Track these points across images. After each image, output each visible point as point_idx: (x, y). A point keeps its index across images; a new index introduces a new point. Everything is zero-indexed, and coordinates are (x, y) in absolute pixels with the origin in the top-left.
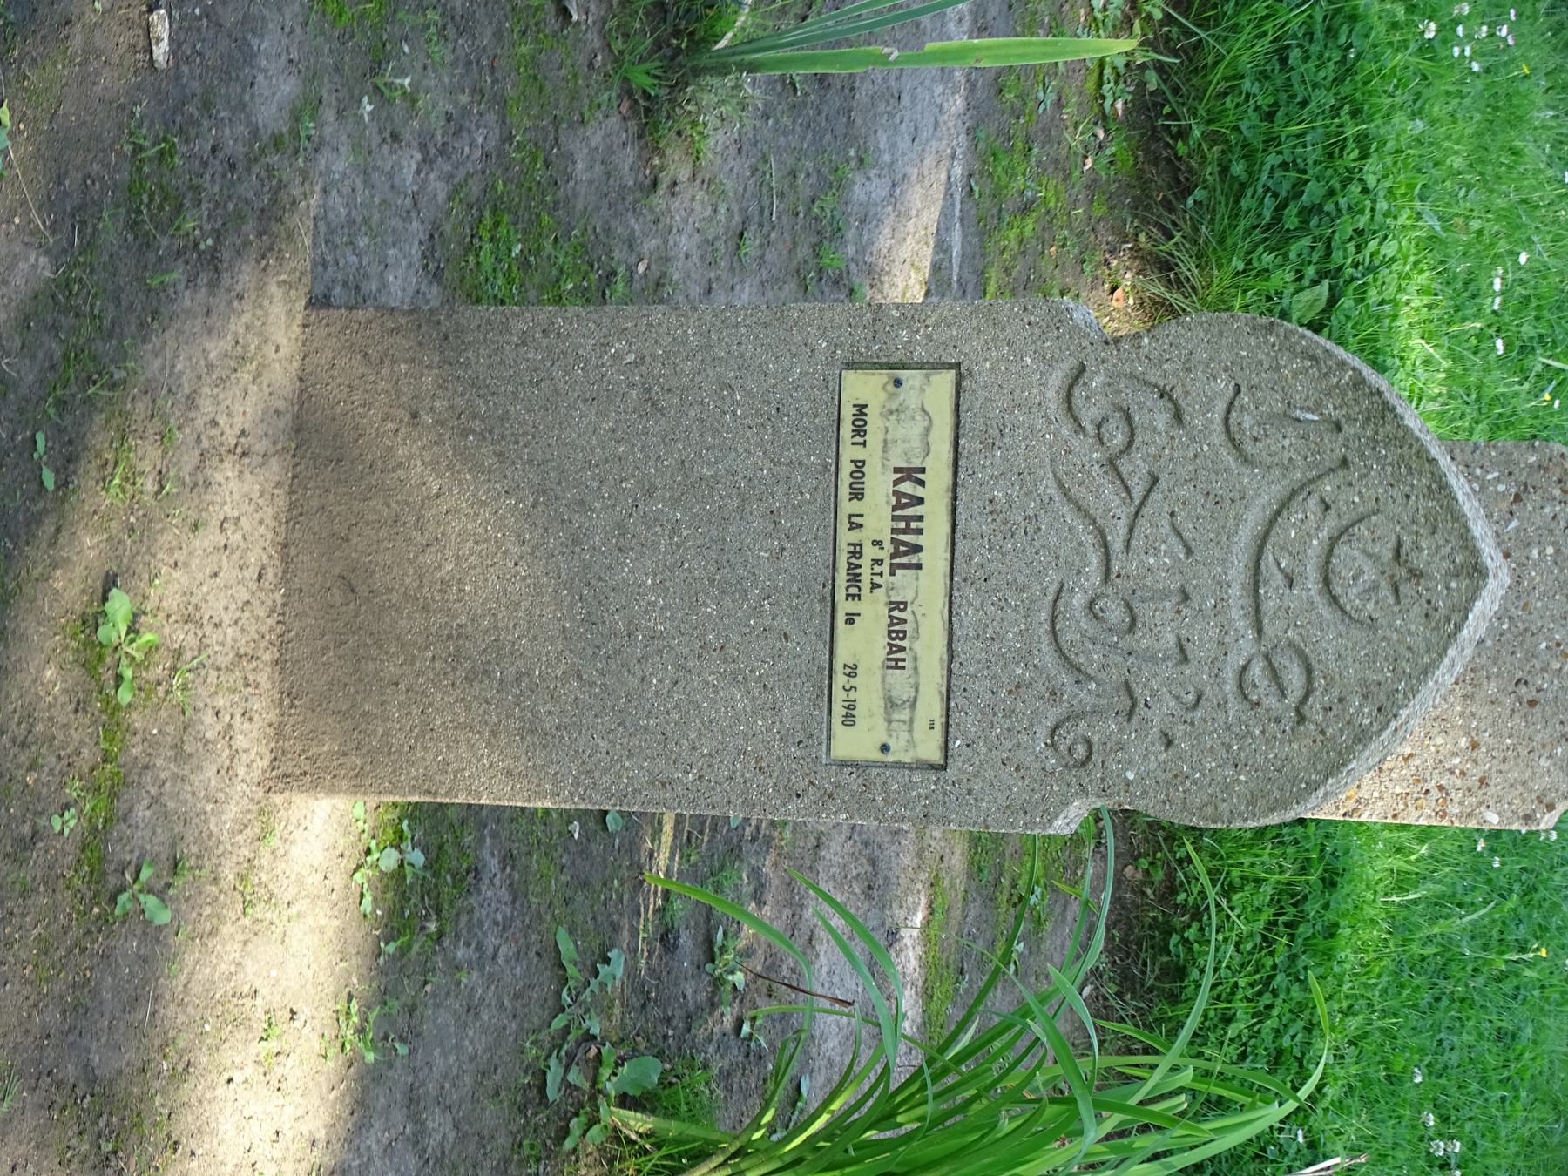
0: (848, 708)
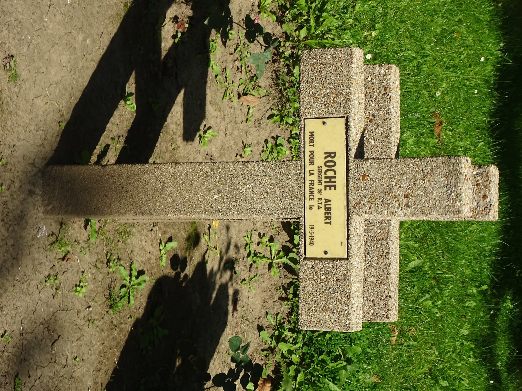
0: (311, 239)
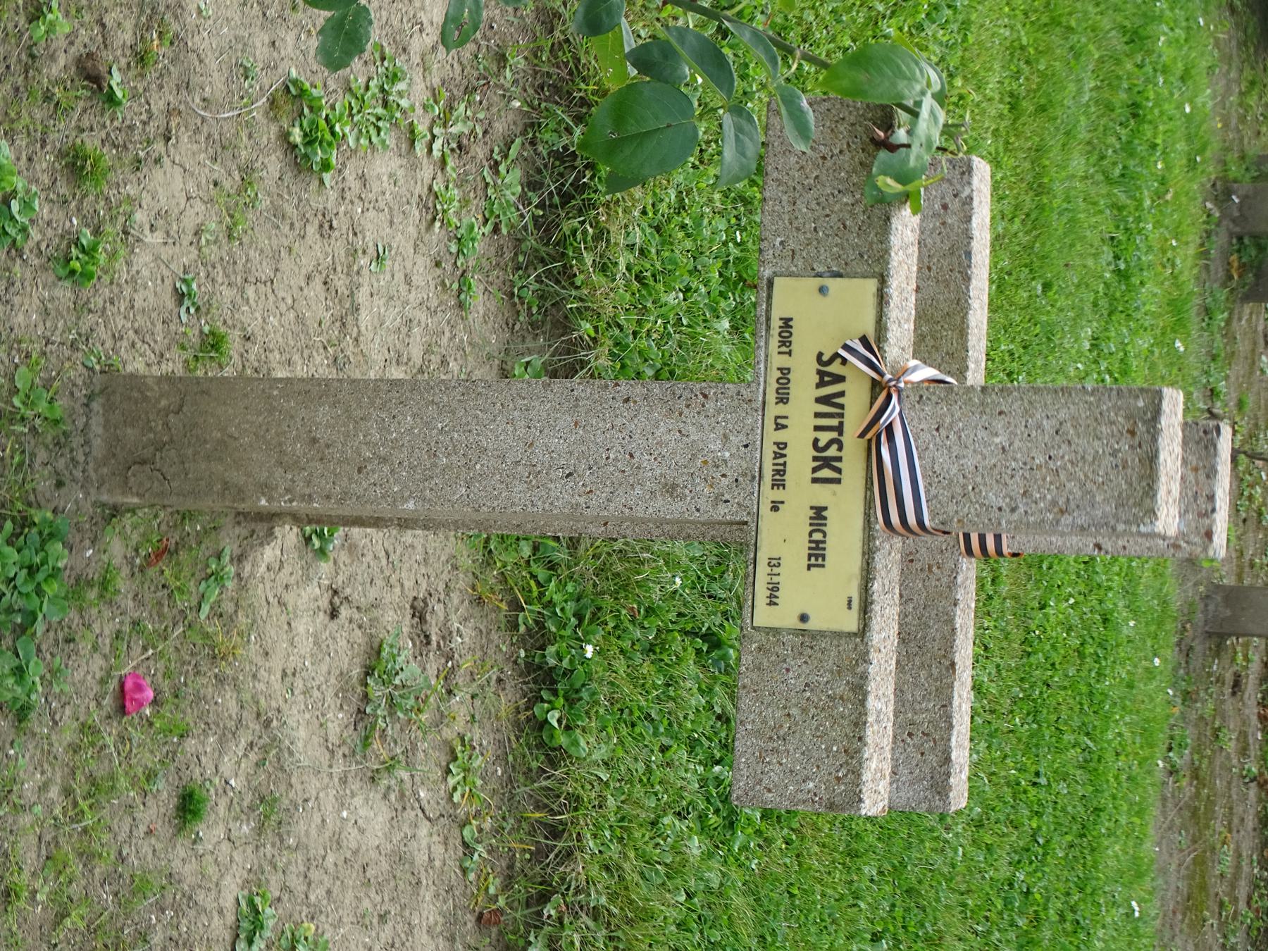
0: (772, 590)
